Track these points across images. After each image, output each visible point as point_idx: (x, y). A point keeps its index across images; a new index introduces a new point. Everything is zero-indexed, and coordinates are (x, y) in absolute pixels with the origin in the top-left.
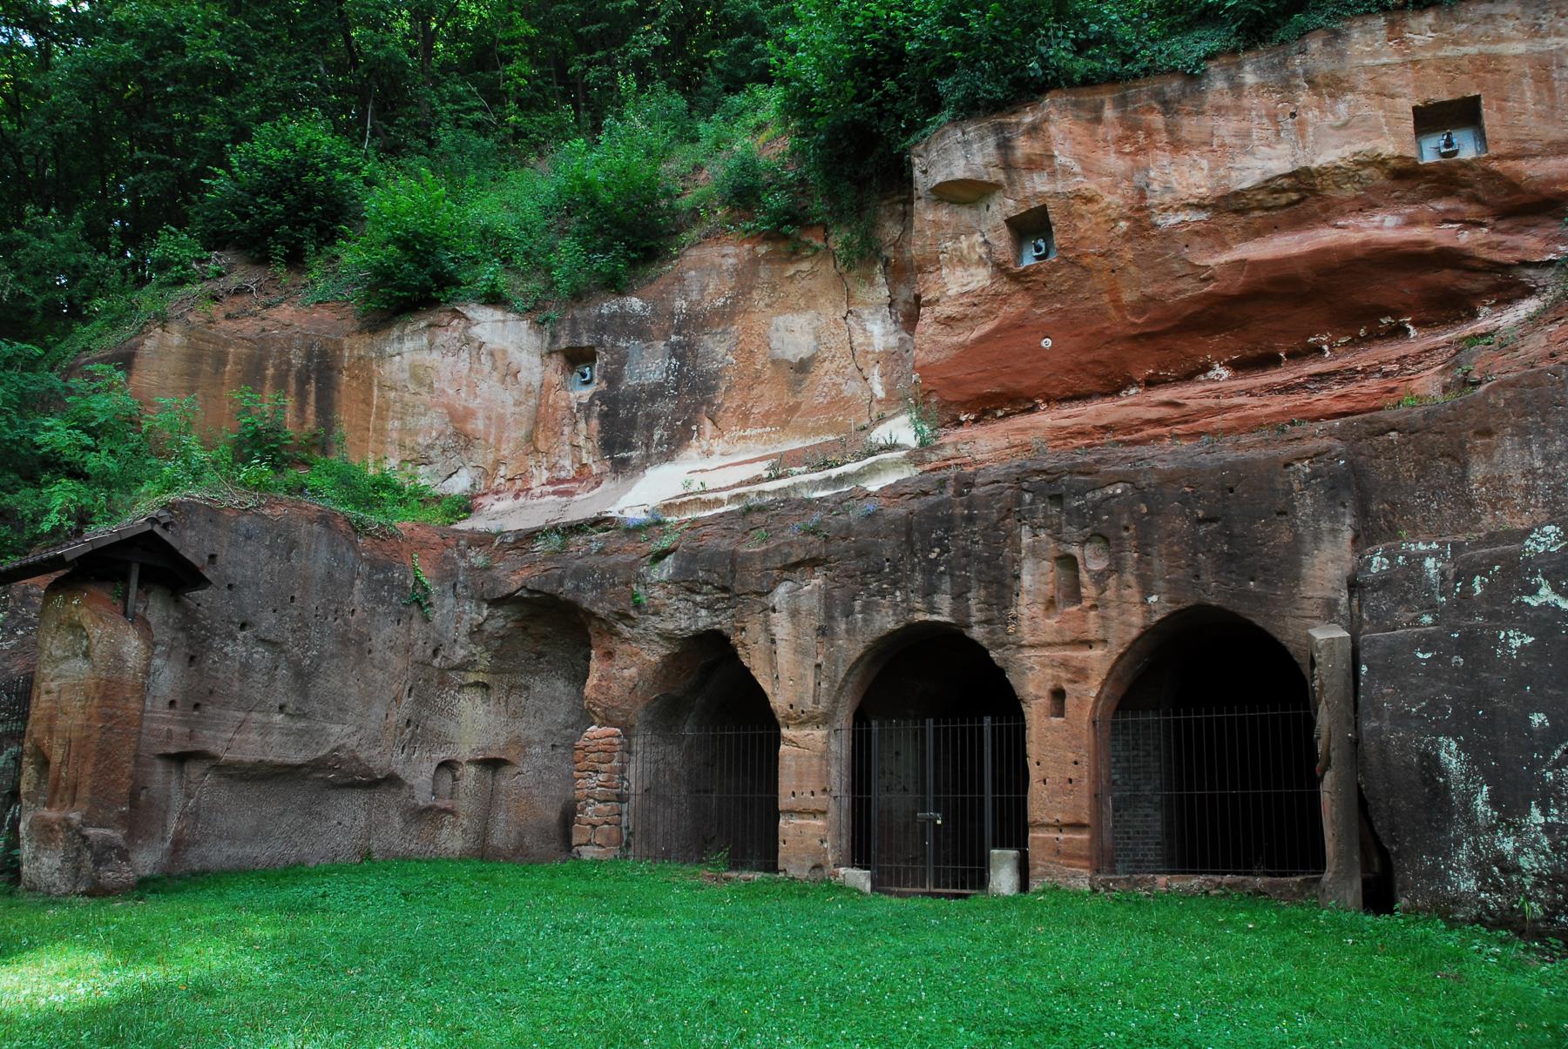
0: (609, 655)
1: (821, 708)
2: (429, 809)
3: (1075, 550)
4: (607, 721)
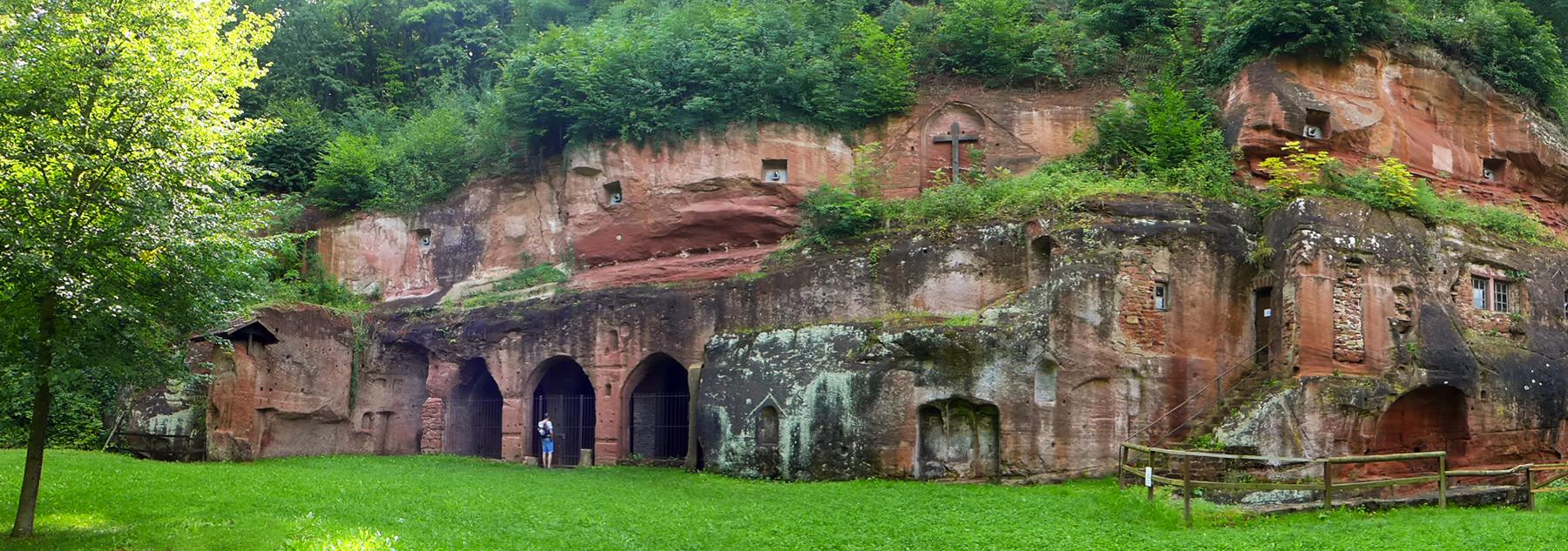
0: (437, 367)
1: (519, 390)
2: (360, 433)
3: (617, 329)
4: (435, 396)
